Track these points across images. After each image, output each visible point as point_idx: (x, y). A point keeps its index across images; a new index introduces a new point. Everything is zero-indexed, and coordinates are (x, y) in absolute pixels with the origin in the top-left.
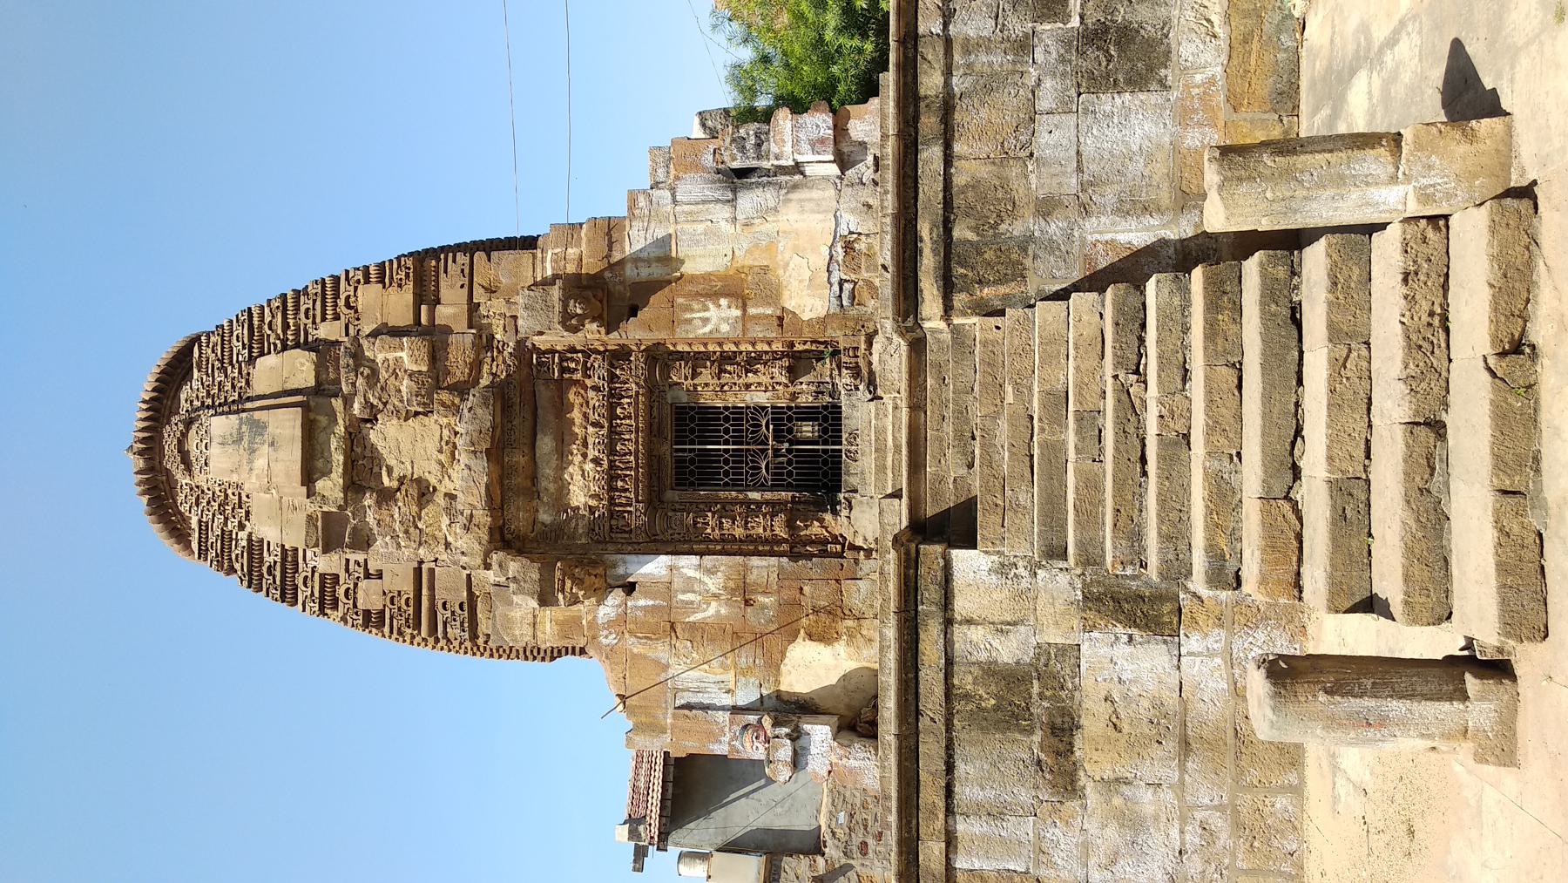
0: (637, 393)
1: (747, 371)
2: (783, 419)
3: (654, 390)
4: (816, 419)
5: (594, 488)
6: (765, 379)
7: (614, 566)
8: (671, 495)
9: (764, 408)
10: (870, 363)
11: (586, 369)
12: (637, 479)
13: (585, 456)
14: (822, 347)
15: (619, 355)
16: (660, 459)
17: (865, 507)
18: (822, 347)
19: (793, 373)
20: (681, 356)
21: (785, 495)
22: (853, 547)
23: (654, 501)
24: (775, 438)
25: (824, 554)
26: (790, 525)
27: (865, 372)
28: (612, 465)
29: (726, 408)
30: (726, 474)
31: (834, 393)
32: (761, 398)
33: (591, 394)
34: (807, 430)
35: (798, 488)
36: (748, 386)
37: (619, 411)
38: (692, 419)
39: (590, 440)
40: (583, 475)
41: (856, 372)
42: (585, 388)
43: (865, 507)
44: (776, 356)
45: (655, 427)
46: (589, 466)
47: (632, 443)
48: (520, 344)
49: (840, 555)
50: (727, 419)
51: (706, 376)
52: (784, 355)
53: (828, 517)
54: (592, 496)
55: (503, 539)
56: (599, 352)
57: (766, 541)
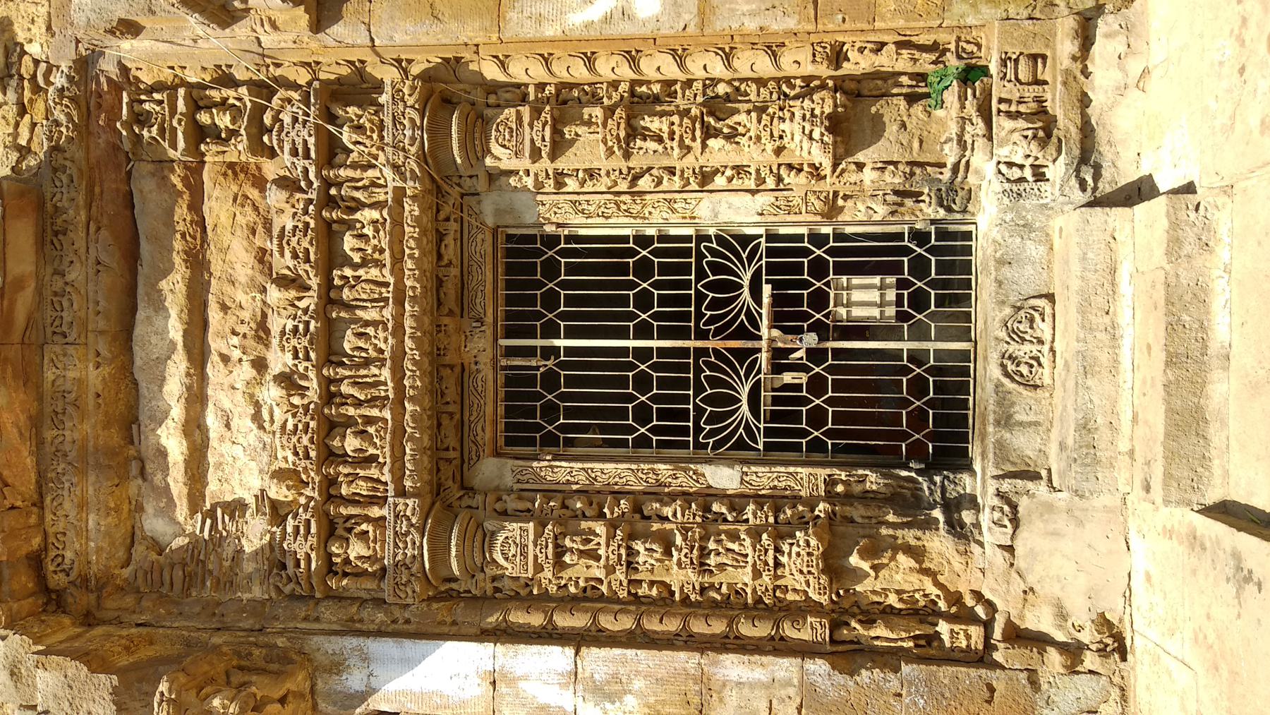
0: (400, 193)
1: (709, 133)
2: (798, 272)
3: (449, 189)
4: (895, 269)
5: (286, 458)
6: (754, 155)
7: (337, 666)
8: (492, 470)
9: (745, 240)
10: (1084, 101)
11: (258, 129)
12: (399, 431)
13: (260, 365)
14: (925, 63)
15: (355, 89)
16: (463, 373)
17: (1061, 522)
18: (925, 63)
19: (848, 129)
20: (518, 93)
21: (806, 478)
22: (1017, 636)
23: (450, 493)
24: (777, 320)
25: (930, 651)
26: (834, 568)
27: (1067, 123)
28: (330, 396)
29: (644, 241)
30: (643, 415)
31: (954, 194)
32: (736, 211)
33: (276, 197)
34: (865, 298)
35: (853, 452)
36: (706, 177)
37: (349, 242)
38: (551, 269)
39: (276, 324)
40: (257, 417)
41: (1044, 127)
42: (260, 183)
43: (1061, 522)
44: (787, 90)
45: (450, 288)
46: (272, 394)
47: (384, 328)
48: (85, 65)
49: (981, 658)
50: (644, 269)
51: (590, 146)
52: (810, 87)
53: (939, 544)
54: (279, 475)
55: (43, 587)
56: (295, 86)
57: (758, 609)
